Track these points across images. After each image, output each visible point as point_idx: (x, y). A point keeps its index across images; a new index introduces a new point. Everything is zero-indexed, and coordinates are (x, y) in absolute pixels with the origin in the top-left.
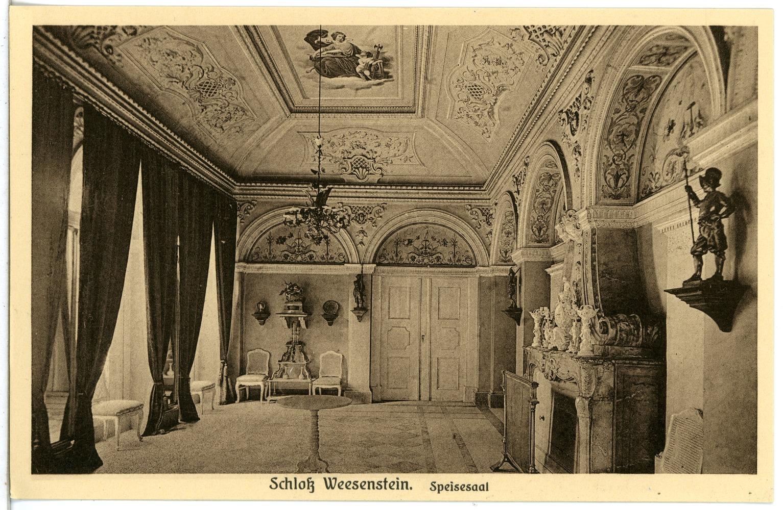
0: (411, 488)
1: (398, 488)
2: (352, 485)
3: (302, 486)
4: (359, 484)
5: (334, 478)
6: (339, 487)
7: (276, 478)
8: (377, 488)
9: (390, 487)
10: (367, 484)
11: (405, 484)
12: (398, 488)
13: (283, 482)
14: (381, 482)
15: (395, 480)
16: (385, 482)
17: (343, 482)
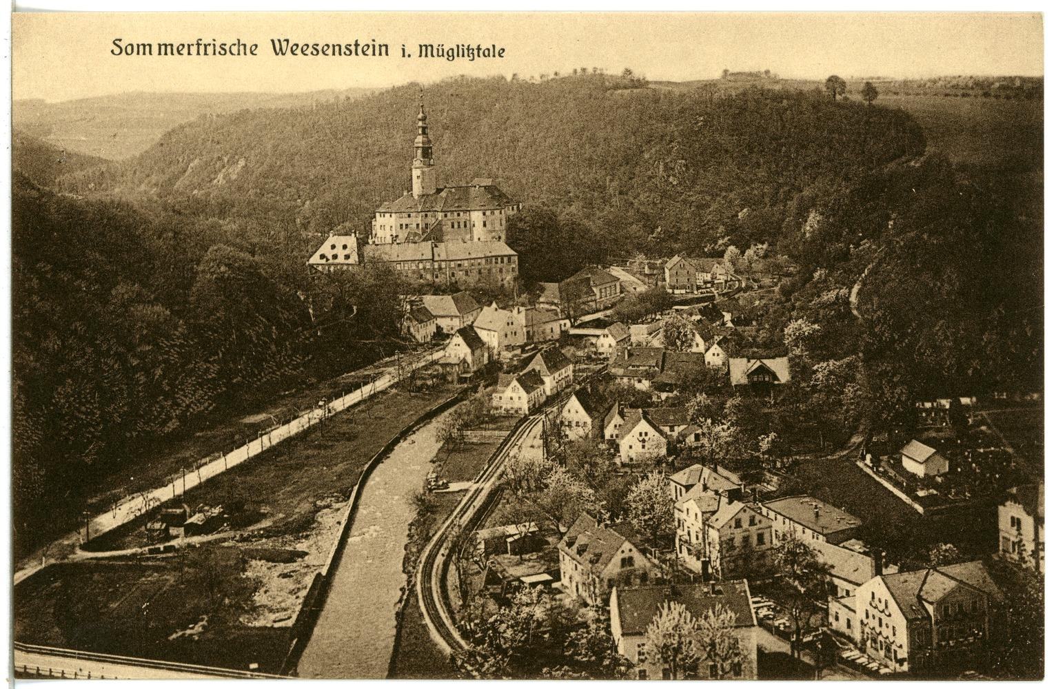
0: (409, 56)
1: (374, 54)
2: (310, 49)
3: (129, 51)
4: (319, 48)
5: (285, 40)
6: (293, 52)
7: (120, 40)
8: (345, 53)
9: (364, 53)
10: (331, 48)
11: (383, 49)
12: (374, 54)
13: (235, 45)
14: (350, 45)
15: (371, 43)
16: (357, 45)
17: (297, 45)
